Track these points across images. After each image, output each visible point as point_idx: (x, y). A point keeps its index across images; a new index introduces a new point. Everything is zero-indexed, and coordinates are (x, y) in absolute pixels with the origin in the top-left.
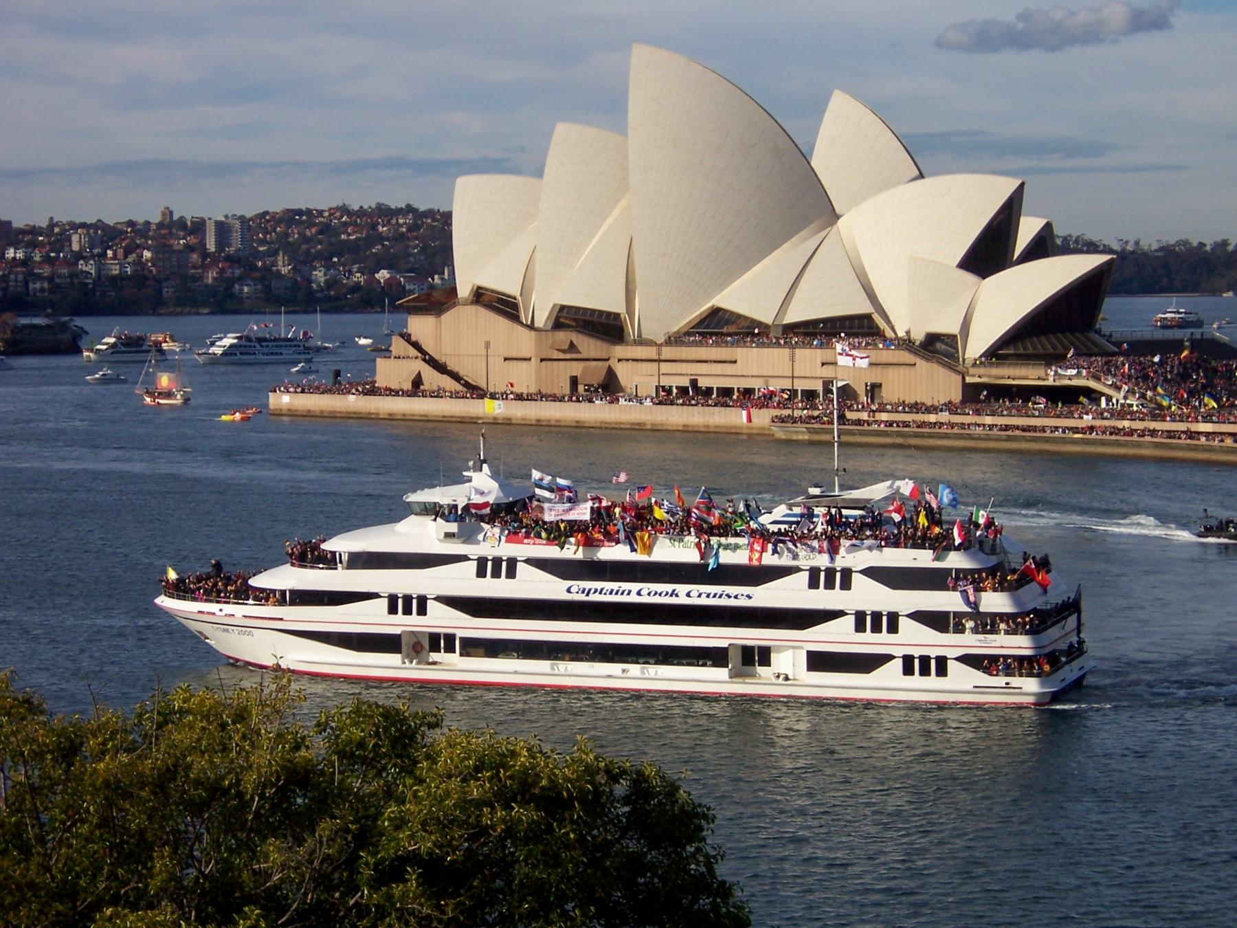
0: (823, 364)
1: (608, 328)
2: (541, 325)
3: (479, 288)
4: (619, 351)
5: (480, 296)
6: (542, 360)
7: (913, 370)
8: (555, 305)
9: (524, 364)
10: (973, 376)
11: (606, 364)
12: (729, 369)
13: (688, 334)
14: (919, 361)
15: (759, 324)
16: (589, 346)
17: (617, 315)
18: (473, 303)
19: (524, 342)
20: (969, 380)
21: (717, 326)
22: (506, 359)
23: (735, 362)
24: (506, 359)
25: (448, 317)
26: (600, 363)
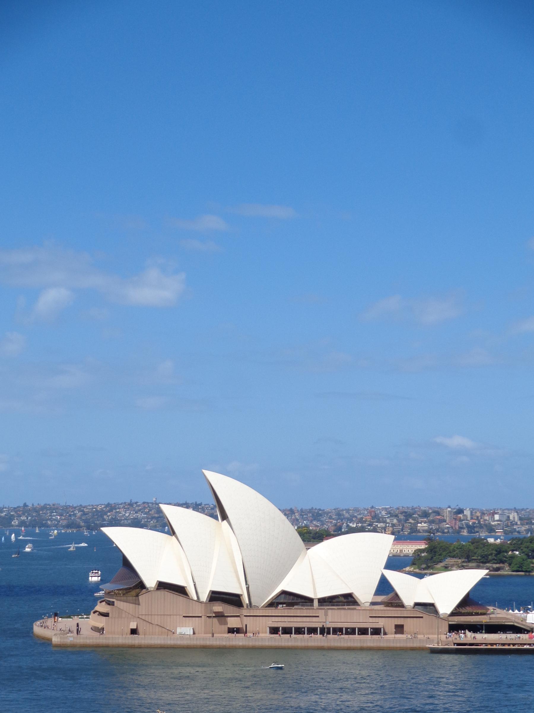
0: (371, 617)
1: (234, 600)
5: (162, 586)
8: (210, 591)
9: (200, 618)
12: (314, 619)
16: (228, 609)
17: (238, 596)
20: (450, 623)
22: (184, 617)
23: (318, 616)
24: (184, 617)
26: (236, 618)
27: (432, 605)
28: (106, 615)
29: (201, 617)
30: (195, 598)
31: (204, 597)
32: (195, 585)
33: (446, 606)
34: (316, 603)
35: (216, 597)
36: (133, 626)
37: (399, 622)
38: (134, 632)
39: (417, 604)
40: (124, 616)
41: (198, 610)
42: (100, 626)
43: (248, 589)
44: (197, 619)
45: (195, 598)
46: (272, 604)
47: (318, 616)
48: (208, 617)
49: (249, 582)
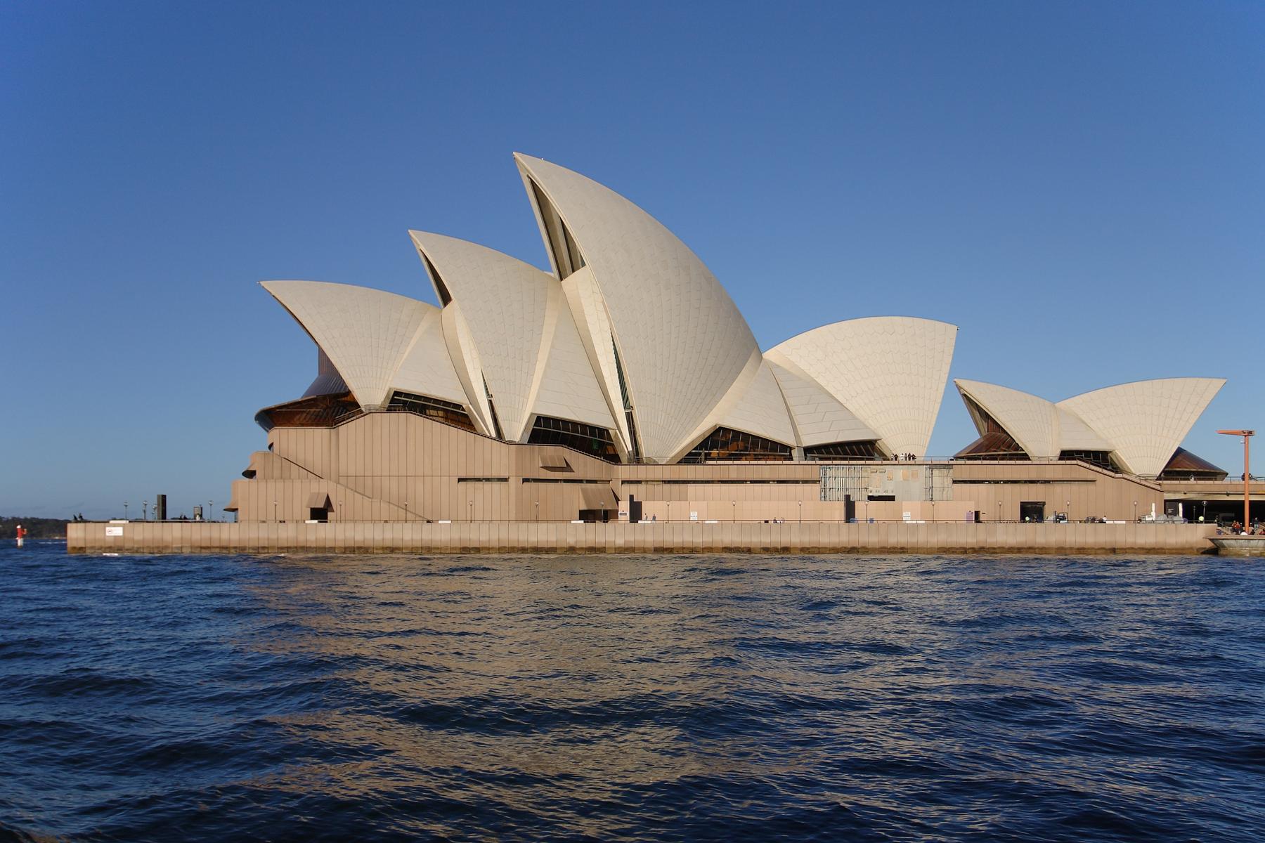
2: (517, 440)
3: (396, 393)
4: (624, 471)
5: (402, 402)
6: (525, 480)
7: (1091, 486)
10: (1175, 492)
11: (607, 486)
13: (690, 454)
14: (1099, 477)
15: (775, 444)
17: (603, 432)
18: (389, 410)
19: (500, 460)
21: (725, 444)
22: (460, 480)
24: (460, 480)
25: (350, 430)
27: (1105, 454)
29: (506, 480)
31: (517, 429)
32: (490, 402)
33: (1145, 456)
35: (547, 431)
37: (1032, 494)
39: (1066, 455)
41: (500, 460)
44: (496, 485)
45: (494, 435)
46: (691, 458)
48: (525, 480)
49: (633, 401)
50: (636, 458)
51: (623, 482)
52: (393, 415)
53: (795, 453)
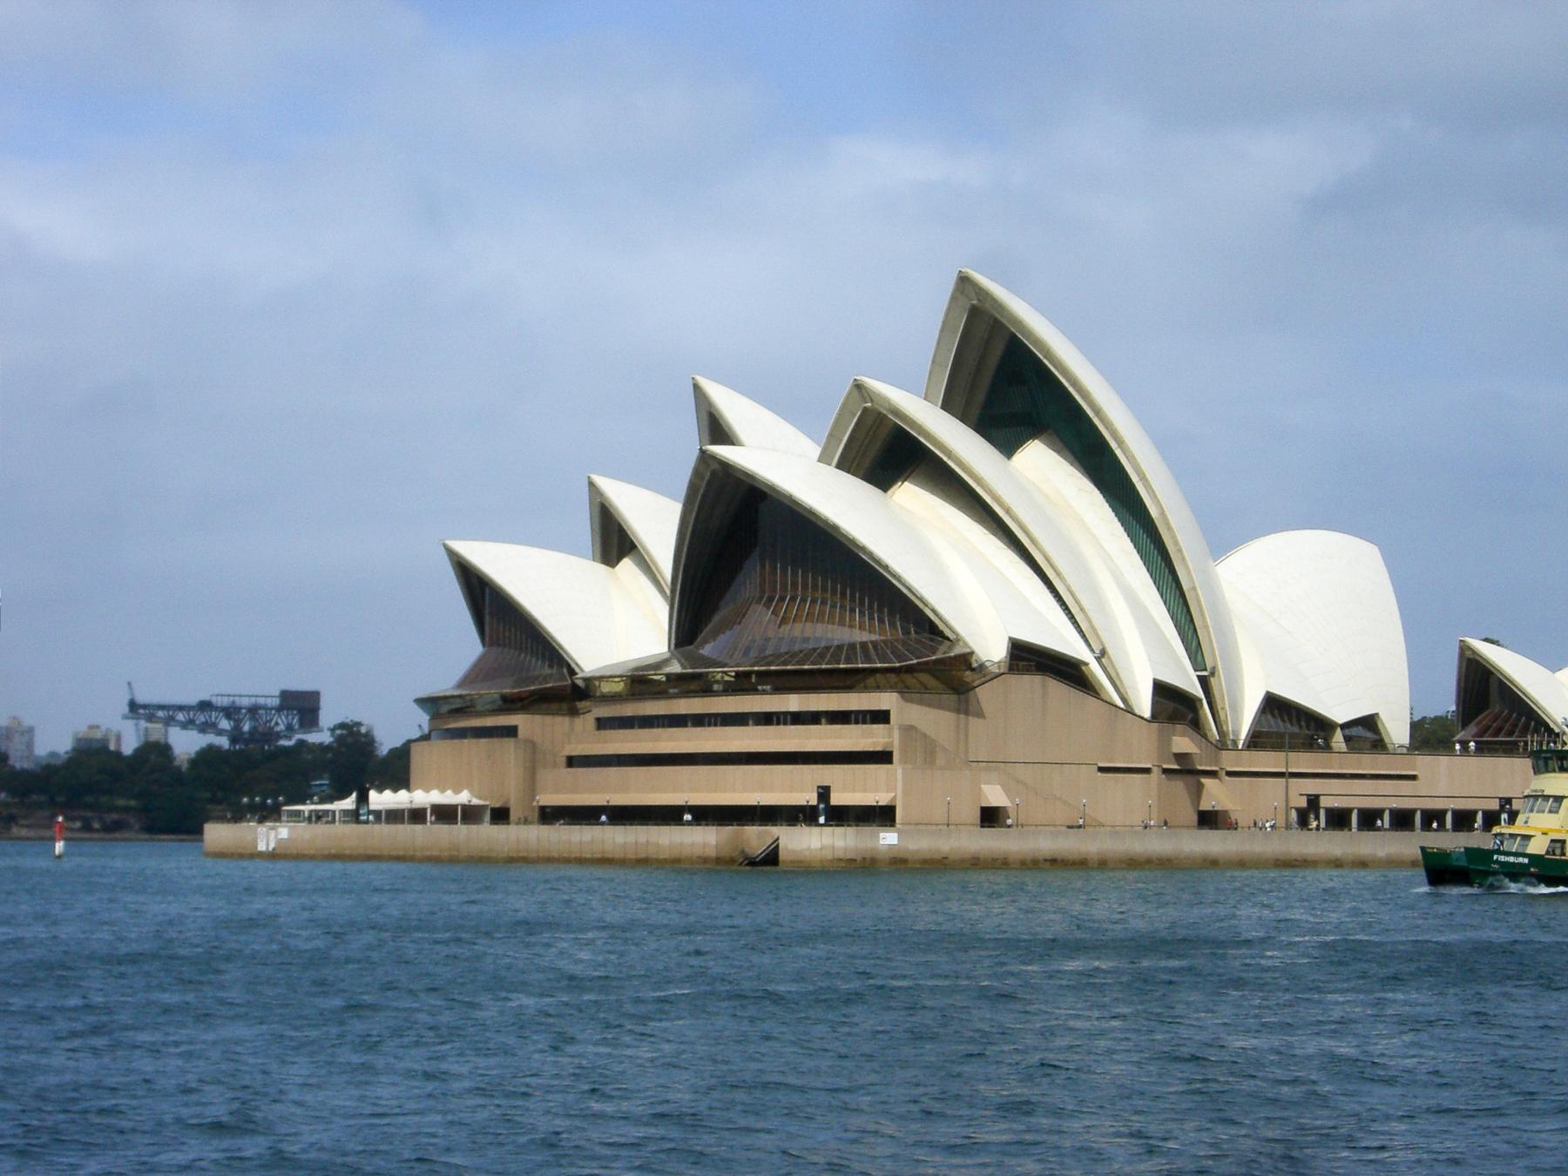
12: (1405, 787)
22: (1101, 770)
23: (1413, 778)
24: (1101, 770)
28: (883, 757)
30: (1121, 704)
31: (1144, 703)
32: (1098, 659)
34: (1338, 739)
36: (995, 796)
38: (991, 817)
40: (940, 761)
42: (883, 799)
43: (1204, 682)
45: (1121, 704)
46: (1257, 740)
47: (1413, 778)
50: (1224, 744)
51: (1230, 774)
52: (1027, 678)
53: (1338, 739)
